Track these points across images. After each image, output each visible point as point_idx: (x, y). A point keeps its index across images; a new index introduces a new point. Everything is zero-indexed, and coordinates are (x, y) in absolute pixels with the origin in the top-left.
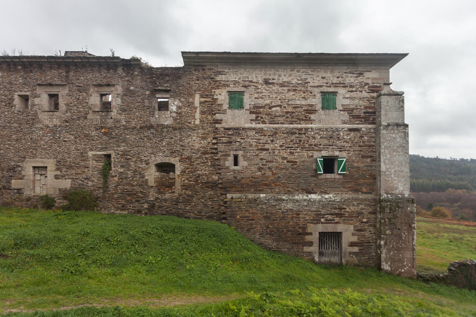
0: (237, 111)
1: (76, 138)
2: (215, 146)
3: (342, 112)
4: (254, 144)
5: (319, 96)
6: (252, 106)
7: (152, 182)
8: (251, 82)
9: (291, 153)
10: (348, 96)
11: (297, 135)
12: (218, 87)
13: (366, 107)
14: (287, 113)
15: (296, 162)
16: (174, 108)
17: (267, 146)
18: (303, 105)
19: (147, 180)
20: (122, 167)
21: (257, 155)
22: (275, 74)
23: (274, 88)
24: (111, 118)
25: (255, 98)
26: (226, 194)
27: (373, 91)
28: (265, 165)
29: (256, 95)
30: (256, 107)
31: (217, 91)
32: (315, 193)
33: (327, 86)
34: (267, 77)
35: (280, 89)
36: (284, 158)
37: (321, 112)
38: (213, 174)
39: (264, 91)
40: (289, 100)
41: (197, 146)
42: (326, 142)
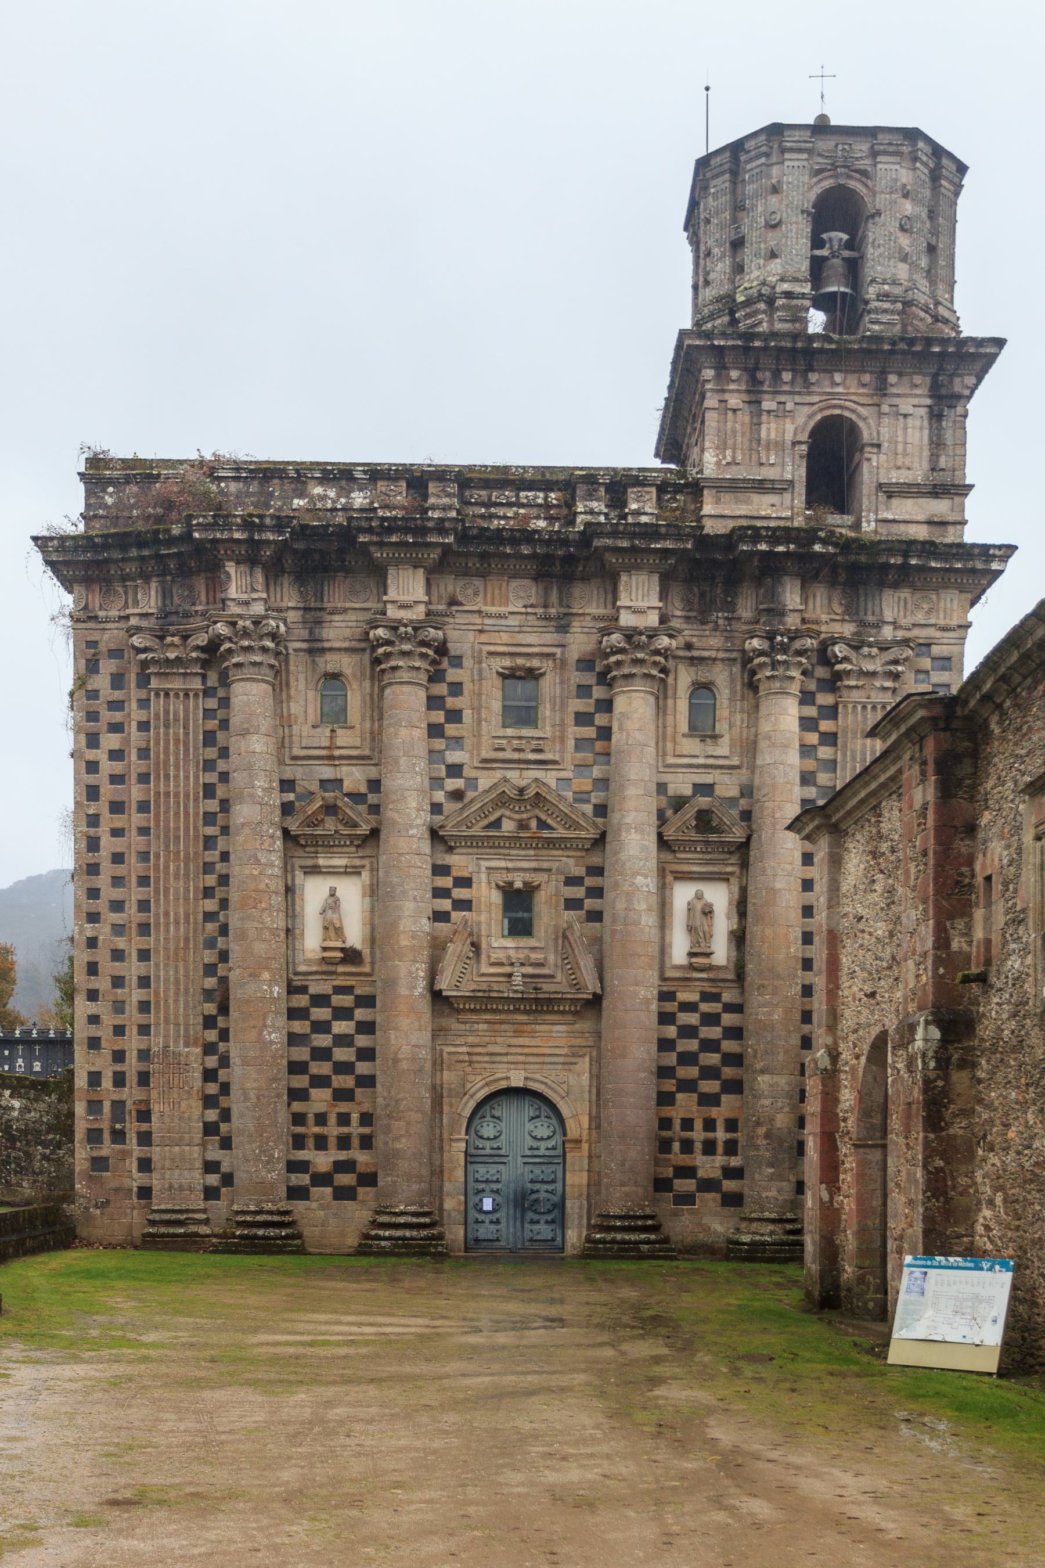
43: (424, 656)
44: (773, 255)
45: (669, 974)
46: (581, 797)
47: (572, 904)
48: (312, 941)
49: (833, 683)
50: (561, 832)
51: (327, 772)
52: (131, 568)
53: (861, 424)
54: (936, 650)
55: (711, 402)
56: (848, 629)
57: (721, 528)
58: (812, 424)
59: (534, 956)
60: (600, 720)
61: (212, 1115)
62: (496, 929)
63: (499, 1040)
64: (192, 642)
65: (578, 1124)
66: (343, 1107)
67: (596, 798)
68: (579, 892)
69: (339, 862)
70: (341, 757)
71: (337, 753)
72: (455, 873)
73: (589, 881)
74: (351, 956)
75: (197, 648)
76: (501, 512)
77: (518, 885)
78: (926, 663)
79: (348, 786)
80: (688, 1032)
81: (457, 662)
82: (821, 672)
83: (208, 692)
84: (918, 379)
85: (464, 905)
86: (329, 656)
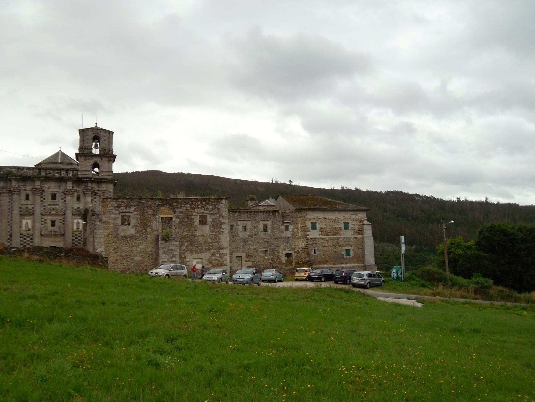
0: (314, 231)
1: (254, 243)
2: (307, 246)
3: (351, 231)
4: (321, 244)
5: (343, 224)
6: (320, 228)
7: (284, 262)
8: (319, 218)
9: (335, 248)
10: (353, 224)
11: (337, 241)
12: (307, 221)
13: (359, 229)
14: (332, 231)
15: (336, 251)
16: (291, 230)
17: (326, 245)
18: (338, 228)
19: (282, 261)
20: (272, 255)
21: (323, 249)
22: (327, 215)
23: (327, 221)
24: (268, 234)
25: (321, 225)
26: (312, 266)
27: (361, 222)
28: (326, 253)
29: (321, 224)
30: (321, 229)
31: (307, 222)
32: (343, 264)
33: (346, 220)
34: (324, 216)
35: (329, 221)
36: (332, 250)
37: (344, 230)
38: (307, 257)
39: (324, 222)
40: (333, 226)
41: (301, 246)
42: (346, 243)
43: (40, 192)
44: (88, 143)
45: (74, 231)
46: (62, 209)
47: (61, 222)
48: (24, 228)
49: (96, 194)
50: (59, 214)
51: (26, 206)
53: (99, 164)
54: (109, 191)
56: (97, 188)
57: (80, 176)
58: (93, 163)
59: (56, 229)
60: (64, 199)
62: (50, 226)
67: (64, 209)
68: (61, 221)
69: (28, 218)
72: (44, 219)
73: (63, 219)
74: (29, 230)
76: (51, 173)
77: (53, 220)
78: (108, 192)
79: (29, 208)
80: (76, 238)
81: (45, 192)
82: (94, 193)
83: (9, 196)
84: (106, 159)
85: (46, 223)
86: (27, 191)
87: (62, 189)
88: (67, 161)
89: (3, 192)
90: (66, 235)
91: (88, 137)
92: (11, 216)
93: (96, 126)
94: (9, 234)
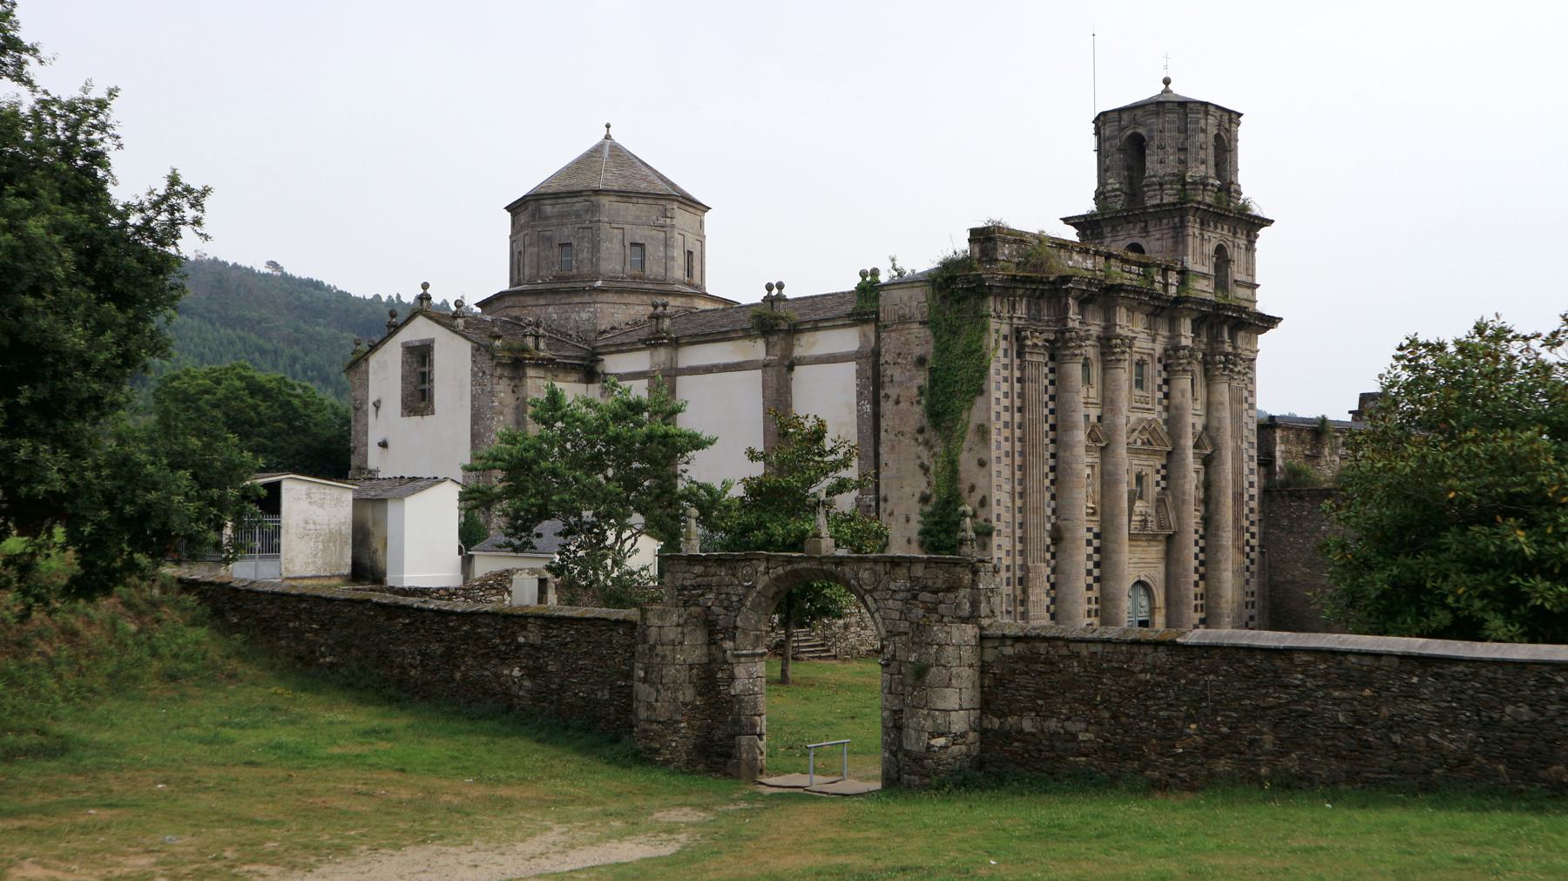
44: (1202, 163)
47: (1158, 484)
52: (1020, 292)
55: (1190, 231)
61: (1048, 601)
63: (1136, 555)
64: (1045, 336)
65: (1160, 599)
66: (1090, 594)
70: (1092, 404)
71: (1090, 400)
73: (1163, 472)
75: (1046, 340)
87: (1159, 348)
88: (643, 187)
89: (1035, 345)
90: (1177, 537)
91: (1202, 136)
92: (1051, 449)
93: (1167, 91)
94: (1048, 526)
